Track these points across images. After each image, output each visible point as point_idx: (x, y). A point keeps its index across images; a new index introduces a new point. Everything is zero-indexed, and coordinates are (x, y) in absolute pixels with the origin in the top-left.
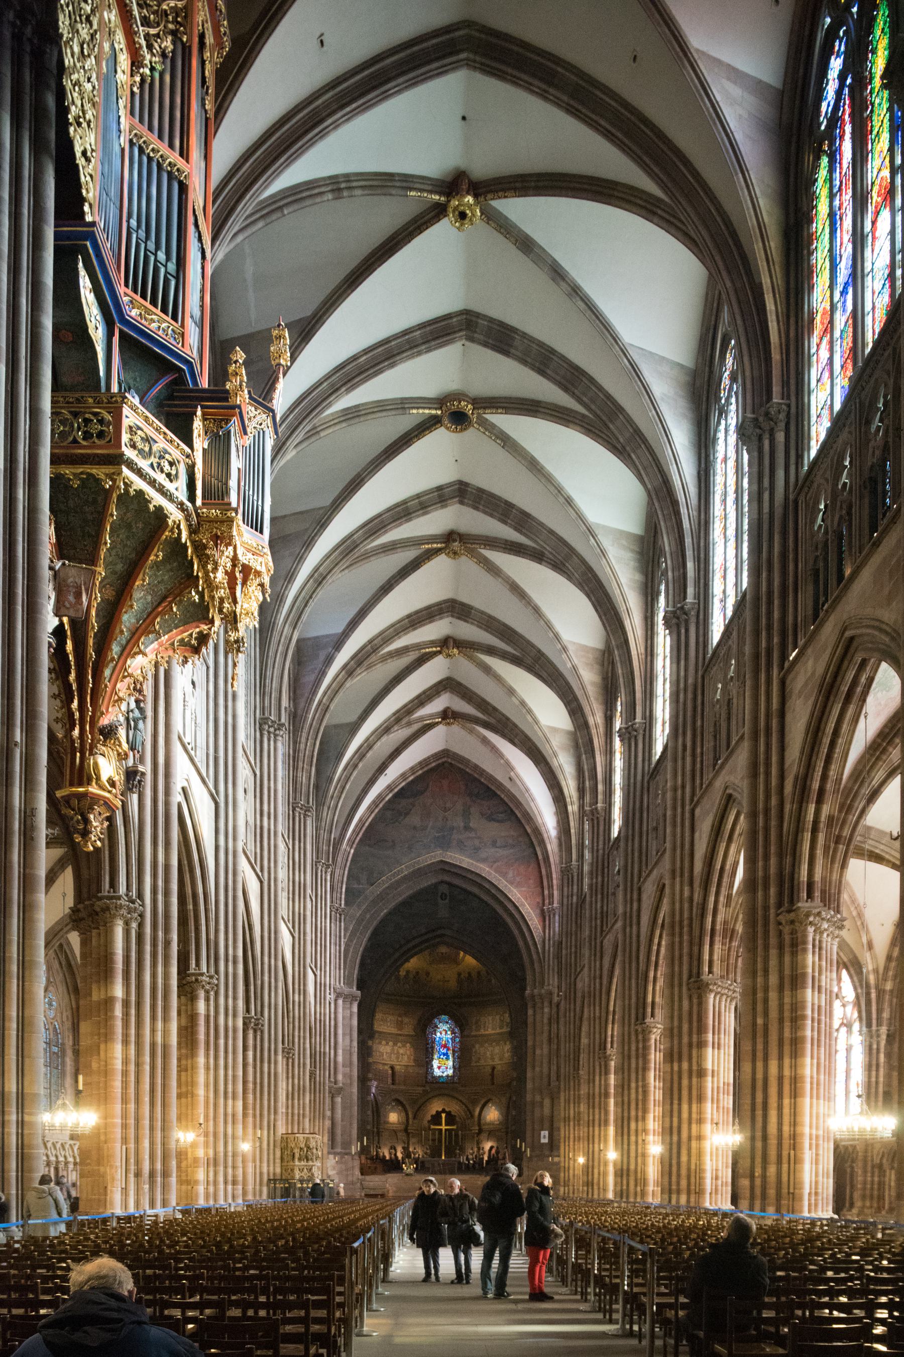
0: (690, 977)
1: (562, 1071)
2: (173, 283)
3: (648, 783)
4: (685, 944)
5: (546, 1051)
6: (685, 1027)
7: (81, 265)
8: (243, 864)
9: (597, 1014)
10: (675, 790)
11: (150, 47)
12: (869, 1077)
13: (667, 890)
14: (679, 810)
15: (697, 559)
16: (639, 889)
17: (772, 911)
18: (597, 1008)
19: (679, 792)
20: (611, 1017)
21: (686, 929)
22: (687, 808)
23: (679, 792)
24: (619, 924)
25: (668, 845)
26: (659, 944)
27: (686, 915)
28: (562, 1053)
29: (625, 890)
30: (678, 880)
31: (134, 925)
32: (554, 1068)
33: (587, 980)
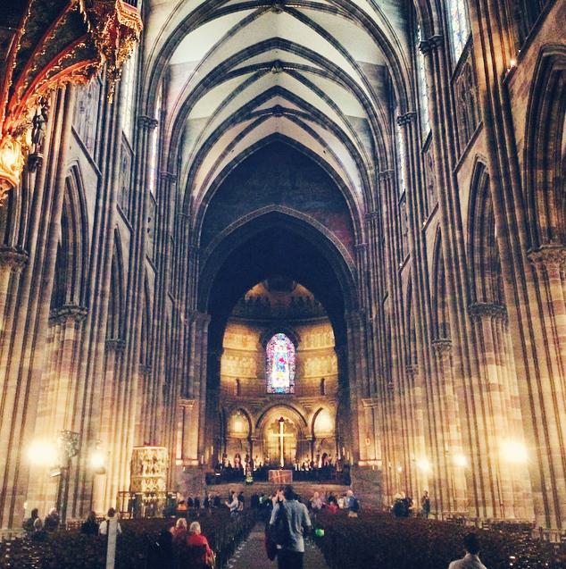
0: (469, 302)
3: (422, 154)
4: (462, 276)
8: (116, 218)
9: (402, 333)
10: (440, 159)
15: (438, 9)
17: (523, 251)
18: (401, 328)
20: (412, 336)
21: (460, 264)
22: (451, 172)
24: (411, 259)
26: (443, 275)
29: (413, 233)
31: (20, 270)
33: (390, 303)
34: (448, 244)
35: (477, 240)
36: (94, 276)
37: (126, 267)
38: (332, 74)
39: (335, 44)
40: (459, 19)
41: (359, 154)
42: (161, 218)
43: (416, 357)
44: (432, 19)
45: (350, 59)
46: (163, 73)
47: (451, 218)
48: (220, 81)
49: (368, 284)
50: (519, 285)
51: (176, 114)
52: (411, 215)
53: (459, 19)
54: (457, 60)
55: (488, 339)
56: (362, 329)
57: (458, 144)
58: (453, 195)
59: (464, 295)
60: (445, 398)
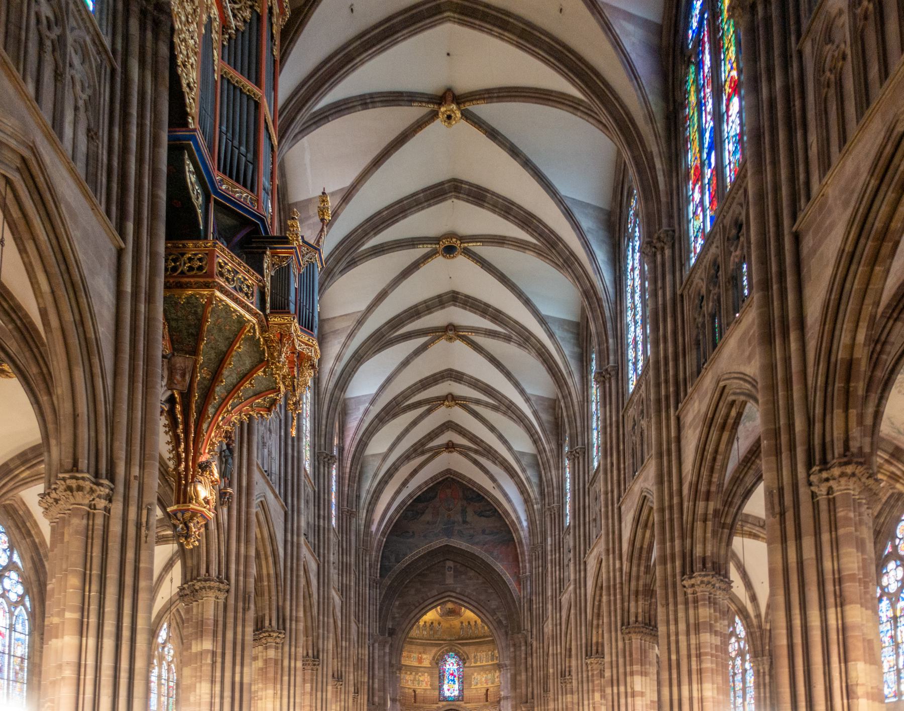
0: (623, 625)
1: (535, 692)
2: (251, 167)
4: (618, 601)
5: (523, 677)
6: (621, 661)
7: (186, 156)
8: (305, 552)
10: (606, 493)
11: (235, 16)
12: (759, 693)
13: (604, 564)
14: (610, 508)
16: (585, 562)
17: (678, 578)
19: (610, 495)
21: (618, 591)
22: (616, 505)
23: (610, 495)
25: (603, 532)
26: (600, 601)
27: (618, 581)
28: (535, 679)
30: (611, 556)
32: (530, 689)
33: (550, 626)
34: (608, 572)
35: (634, 569)
36: (288, 603)
37: (315, 596)
38: (503, 408)
39: (508, 375)
40: (635, 347)
41: (527, 490)
42: (343, 551)
43: (570, 672)
44: (608, 347)
45: (522, 392)
46: (339, 409)
47: (613, 550)
48: (395, 416)
49: (530, 610)
50: (671, 607)
51: (353, 449)
52: (575, 547)
53: (635, 347)
54: (631, 390)
55: (636, 655)
56: (523, 648)
57: (625, 478)
58: (616, 527)
59: (619, 618)
60: (594, 703)
